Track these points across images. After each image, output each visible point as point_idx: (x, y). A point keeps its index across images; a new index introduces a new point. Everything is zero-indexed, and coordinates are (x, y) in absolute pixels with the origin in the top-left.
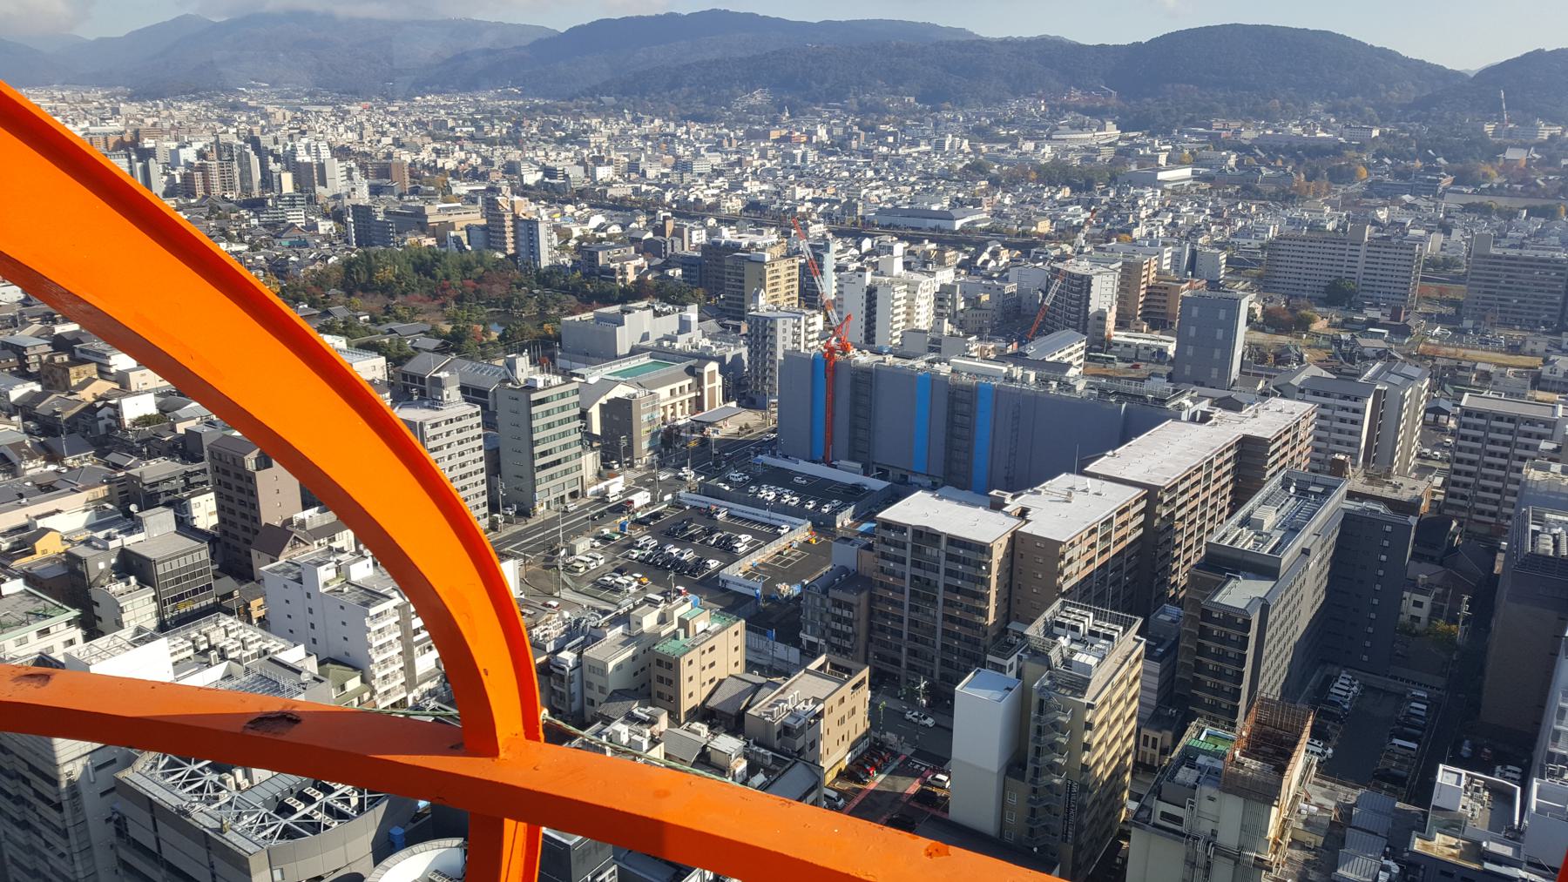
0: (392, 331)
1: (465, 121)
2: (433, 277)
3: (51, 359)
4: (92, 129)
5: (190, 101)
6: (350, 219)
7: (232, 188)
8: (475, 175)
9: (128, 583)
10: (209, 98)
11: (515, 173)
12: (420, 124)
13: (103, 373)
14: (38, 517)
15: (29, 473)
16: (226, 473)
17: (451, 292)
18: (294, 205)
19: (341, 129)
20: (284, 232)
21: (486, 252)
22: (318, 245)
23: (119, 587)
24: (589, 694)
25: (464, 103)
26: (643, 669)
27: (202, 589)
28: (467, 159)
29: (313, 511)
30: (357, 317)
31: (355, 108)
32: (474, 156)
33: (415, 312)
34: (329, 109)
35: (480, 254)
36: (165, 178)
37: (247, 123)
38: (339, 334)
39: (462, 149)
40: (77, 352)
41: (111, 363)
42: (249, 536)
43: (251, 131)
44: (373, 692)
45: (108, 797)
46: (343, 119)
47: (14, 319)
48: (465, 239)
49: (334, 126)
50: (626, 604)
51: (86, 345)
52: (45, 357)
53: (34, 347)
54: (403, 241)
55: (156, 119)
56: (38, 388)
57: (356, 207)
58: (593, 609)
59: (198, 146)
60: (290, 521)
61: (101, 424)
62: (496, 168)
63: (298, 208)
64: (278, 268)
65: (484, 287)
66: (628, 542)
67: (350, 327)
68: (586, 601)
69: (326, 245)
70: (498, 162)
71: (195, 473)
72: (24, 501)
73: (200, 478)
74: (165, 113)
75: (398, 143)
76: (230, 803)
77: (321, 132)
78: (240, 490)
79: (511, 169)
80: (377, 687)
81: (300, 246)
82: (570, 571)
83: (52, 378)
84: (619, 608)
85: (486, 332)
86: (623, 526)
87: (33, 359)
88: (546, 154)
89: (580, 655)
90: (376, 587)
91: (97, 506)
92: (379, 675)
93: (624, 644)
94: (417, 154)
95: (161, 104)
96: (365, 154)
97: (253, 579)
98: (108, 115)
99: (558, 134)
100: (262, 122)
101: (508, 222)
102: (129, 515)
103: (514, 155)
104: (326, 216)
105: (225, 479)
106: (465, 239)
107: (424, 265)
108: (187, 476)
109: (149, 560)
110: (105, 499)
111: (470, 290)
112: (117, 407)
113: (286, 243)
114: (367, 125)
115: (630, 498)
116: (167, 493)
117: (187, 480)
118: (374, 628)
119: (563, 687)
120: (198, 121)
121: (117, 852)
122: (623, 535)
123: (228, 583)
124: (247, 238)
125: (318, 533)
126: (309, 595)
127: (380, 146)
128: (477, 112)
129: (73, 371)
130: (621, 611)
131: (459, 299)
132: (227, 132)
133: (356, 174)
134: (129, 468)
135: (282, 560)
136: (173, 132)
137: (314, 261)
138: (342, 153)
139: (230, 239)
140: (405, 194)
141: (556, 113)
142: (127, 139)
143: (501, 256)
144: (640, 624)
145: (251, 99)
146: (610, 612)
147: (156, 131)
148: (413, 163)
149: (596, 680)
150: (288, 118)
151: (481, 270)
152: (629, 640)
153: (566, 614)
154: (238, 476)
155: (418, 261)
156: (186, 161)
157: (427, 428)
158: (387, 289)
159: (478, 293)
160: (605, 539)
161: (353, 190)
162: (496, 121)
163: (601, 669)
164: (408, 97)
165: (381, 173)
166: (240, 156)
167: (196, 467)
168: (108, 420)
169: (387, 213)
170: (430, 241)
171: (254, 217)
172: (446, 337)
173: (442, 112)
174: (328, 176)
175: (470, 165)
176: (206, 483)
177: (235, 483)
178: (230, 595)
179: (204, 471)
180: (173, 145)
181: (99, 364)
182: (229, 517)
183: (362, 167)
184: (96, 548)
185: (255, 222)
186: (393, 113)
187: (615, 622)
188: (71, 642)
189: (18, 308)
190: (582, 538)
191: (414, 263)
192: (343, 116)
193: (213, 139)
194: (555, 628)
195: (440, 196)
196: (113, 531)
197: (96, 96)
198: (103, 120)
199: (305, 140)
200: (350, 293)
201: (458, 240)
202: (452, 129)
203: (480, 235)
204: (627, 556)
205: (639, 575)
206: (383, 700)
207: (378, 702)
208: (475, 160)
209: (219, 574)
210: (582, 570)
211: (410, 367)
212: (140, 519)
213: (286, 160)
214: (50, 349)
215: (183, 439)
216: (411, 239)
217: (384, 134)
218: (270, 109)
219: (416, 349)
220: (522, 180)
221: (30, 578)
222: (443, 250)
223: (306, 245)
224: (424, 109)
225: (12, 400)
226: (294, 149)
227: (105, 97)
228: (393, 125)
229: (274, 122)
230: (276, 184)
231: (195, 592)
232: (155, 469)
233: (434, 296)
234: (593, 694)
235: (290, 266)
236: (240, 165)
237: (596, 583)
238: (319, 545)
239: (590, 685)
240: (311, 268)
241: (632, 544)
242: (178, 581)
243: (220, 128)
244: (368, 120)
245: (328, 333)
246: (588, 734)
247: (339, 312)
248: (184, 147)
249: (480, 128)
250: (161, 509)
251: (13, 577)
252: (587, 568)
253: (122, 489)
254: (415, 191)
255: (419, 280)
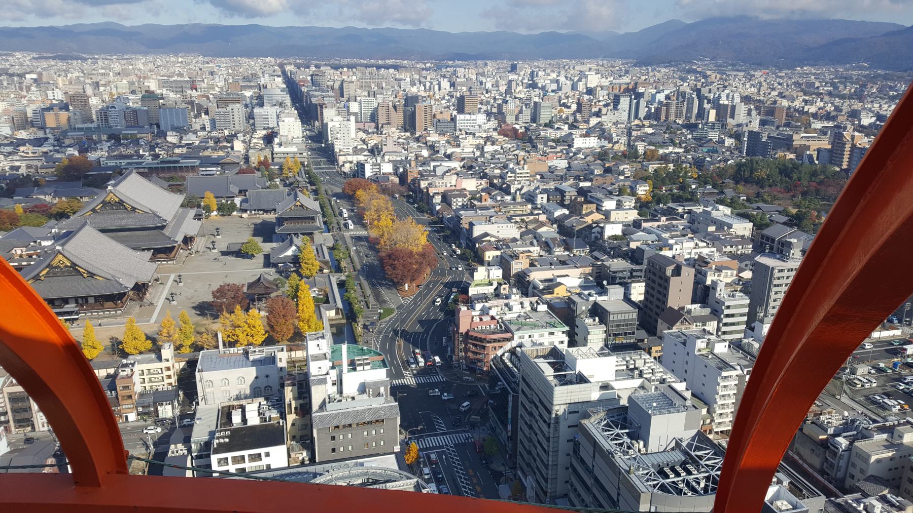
0: (758, 208)
1: (827, 83)
2: (790, 178)
3: (576, 199)
4: (614, 81)
5: (665, 68)
6: (745, 139)
7: (680, 117)
8: (828, 117)
9: (594, 320)
10: (676, 66)
11: (855, 117)
12: (797, 84)
13: (598, 210)
14: (558, 276)
15: (556, 253)
16: (654, 274)
17: (800, 189)
18: (714, 129)
19: (748, 85)
20: (705, 143)
21: (829, 166)
22: (723, 153)
23: (589, 321)
24: (851, 470)
25: (827, 71)
26: (896, 468)
27: (629, 334)
28: (824, 107)
29: (696, 306)
30: (739, 197)
31: (758, 74)
32: (830, 105)
33: (775, 198)
34: (742, 74)
35: (824, 167)
36: (647, 109)
37: (695, 81)
38: (727, 205)
39: (822, 100)
40: (588, 197)
41: (604, 205)
42: (659, 311)
43: (696, 85)
44: (712, 420)
45: (570, 429)
46: (750, 80)
47: (562, 176)
48: (815, 156)
49: (744, 84)
50: (892, 421)
51: (593, 194)
52: (573, 198)
53: (569, 192)
54: (775, 155)
55: (647, 77)
56: (567, 212)
57: (750, 132)
58: (866, 415)
59: (666, 92)
60: (683, 308)
61: (593, 235)
62: (843, 113)
63: (716, 130)
64: (699, 164)
65: (822, 188)
66: (897, 376)
67: (734, 203)
68: (860, 409)
69: (728, 153)
70: (845, 109)
71: (636, 271)
72: (553, 267)
73: (638, 274)
74: (651, 74)
75: (781, 95)
76: (635, 458)
77: (736, 87)
78: (660, 285)
79: (854, 115)
80: (715, 418)
81: (712, 152)
82: (850, 384)
83: (575, 208)
84: (887, 421)
85: (819, 217)
86: (895, 365)
87: (567, 197)
88: (880, 106)
89: (851, 443)
90: (728, 360)
91: (585, 277)
92: (718, 412)
93: (887, 447)
94: (792, 102)
95: (650, 69)
96: (760, 101)
97: (655, 335)
98: (622, 74)
99: (891, 93)
100: (703, 80)
101: (848, 148)
102: (602, 286)
103: (857, 105)
104: (731, 136)
105: (653, 277)
106: (815, 156)
107: (786, 170)
108: (632, 271)
109: (607, 311)
110: (589, 274)
111: (813, 189)
112: (603, 228)
113: (705, 150)
114: (764, 84)
115: (905, 347)
116: (620, 278)
117: (631, 273)
118: (722, 384)
119: (834, 460)
120: (668, 78)
121: (571, 459)
122: (894, 371)
123: (642, 334)
124: (683, 145)
125: (696, 319)
126: (688, 354)
127: (770, 96)
128: (836, 78)
129: (585, 206)
130: (888, 424)
131: (804, 194)
132: (682, 85)
133: (754, 113)
134: (603, 261)
135: (675, 329)
136: (655, 84)
137: (720, 161)
138: (746, 99)
139: (675, 145)
140: (781, 126)
141: (892, 80)
142: (630, 87)
143: (838, 169)
144: (901, 437)
145: (699, 67)
146: (878, 422)
147: (646, 83)
148: (789, 108)
149: (860, 464)
150: (718, 78)
151: (822, 177)
152: (889, 446)
153: (846, 414)
154: (661, 278)
155: (782, 168)
156: (659, 100)
157: (776, 271)
158: (760, 183)
159: (817, 191)
160: (880, 370)
161: (750, 122)
162: (848, 84)
163: (865, 458)
164: (792, 68)
165: (768, 112)
166: (689, 99)
167: (638, 267)
168: (596, 234)
169: (769, 137)
170: (792, 156)
171: (690, 134)
172: (792, 216)
173: (813, 77)
174: (736, 113)
175: (826, 111)
176: (641, 277)
177: (658, 280)
178: (643, 340)
179: (641, 270)
180: (654, 91)
181: (597, 205)
182: (651, 298)
183: (757, 108)
184: (583, 298)
185: (690, 136)
186: (781, 77)
187: (882, 429)
188: (562, 342)
189: (565, 171)
190: (863, 365)
191: (780, 169)
192: (750, 78)
193: (675, 89)
194: (837, 420)
195: (803, 129)
196: (593, 292)
197: (619, 64)
198: (620, 76)
199: (727, 91)
200: (737, 183)
201: (811, 156)
202: (818, 88)
203: (826, 154)
204: (894, 386)
205: (903, 403)
206: (717, 427)
207: (714, 427)
208: (830, 108)
209: (639, 328)
210: (859, 386)
211: (767, 232)
212: (607, 289)
213: (714, 103)
214: (576, 194)
215: (633, 251)
216: (780, 154)
217: (773, 89)
218: (709, 73)
219: (771, 221)
220: (860, 122)
221: (550, 306)
222: (800, 162)
223: (716, 152)
224: (801, 75)
225: (555, 216)
226: (720, 96)
227: (622, 64)
228: (780, 84)
229: (709, 80)
230: (706, 116)
231: (626, 334)
232: (617, 264)
233: (788, 190)
234: (856, 472)
235: (706, 163)
236: (688, 104)
237: (867, 398)
238: (696, 326)
239: (854, 465)
240: (717, 165)
241: (901, 379)
242: (619, 326)
243: (679, 82)
244: (765, 81)
245: (721, 204)
246: (849, 498)
247: (729, 193)
248: (659, 92)
249: (836, 88)
250: (618, 286)
251: (543, 303)
252: (863, 386)
253: (598, 271)
254: (787, 125)
255: (781, 179)
